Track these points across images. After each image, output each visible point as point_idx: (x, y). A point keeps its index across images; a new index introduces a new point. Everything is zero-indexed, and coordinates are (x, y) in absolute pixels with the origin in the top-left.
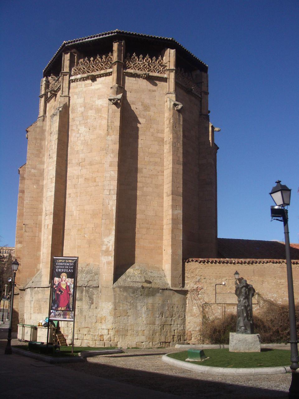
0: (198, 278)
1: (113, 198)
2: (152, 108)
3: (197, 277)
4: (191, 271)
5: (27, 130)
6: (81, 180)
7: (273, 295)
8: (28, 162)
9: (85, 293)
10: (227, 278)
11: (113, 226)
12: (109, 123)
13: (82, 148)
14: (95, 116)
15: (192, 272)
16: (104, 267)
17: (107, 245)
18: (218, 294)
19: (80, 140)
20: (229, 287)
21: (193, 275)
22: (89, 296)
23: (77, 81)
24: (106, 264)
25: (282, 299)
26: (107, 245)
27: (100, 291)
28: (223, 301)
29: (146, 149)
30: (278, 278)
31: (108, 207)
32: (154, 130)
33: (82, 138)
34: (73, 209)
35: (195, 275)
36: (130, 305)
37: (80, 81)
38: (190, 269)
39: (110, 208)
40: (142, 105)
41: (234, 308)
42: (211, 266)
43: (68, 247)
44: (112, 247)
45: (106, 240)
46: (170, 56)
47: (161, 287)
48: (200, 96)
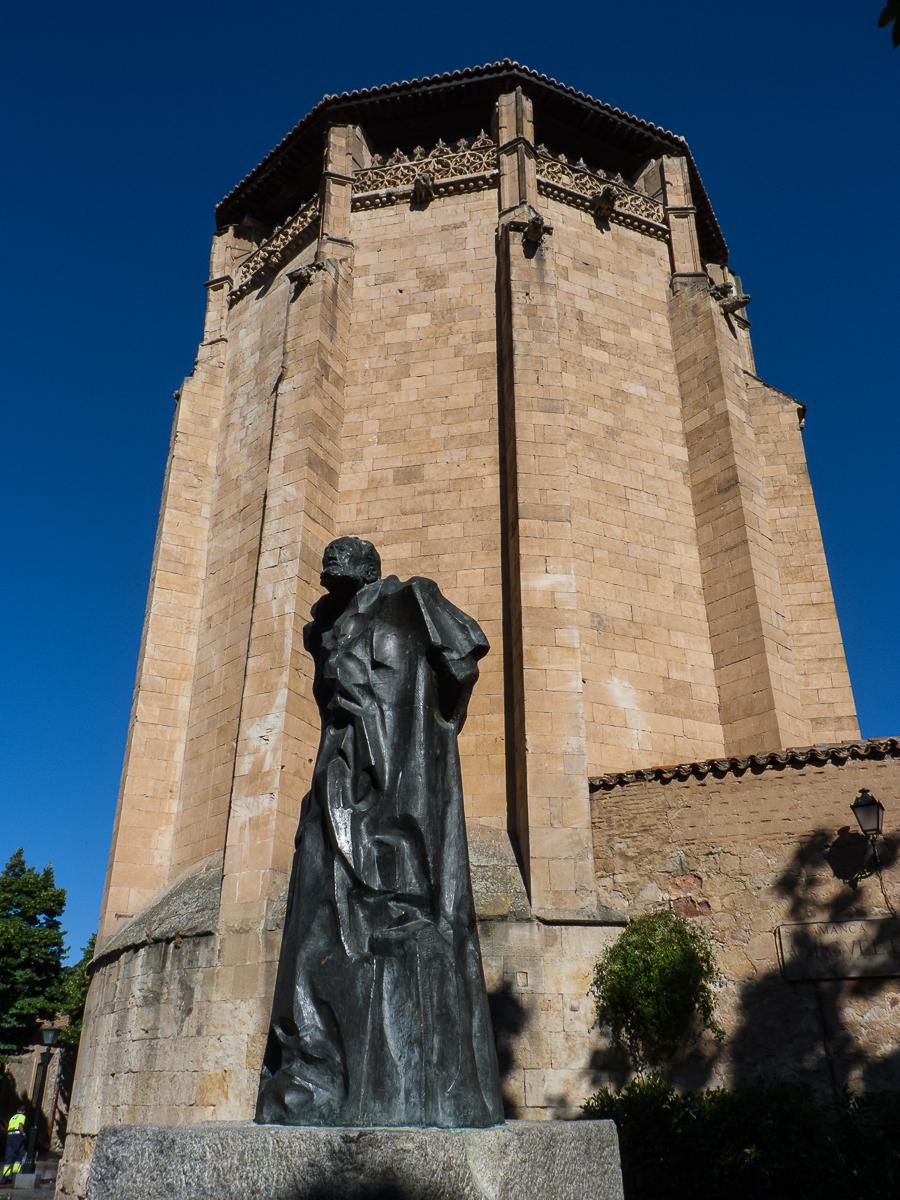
0: (678, 853)
2: (453, 276)
3: (668, 849)
9: (173, 965)
16: (240, 841)
17: (257, 751)
21: (648, 845)
22: (180, 981)
24: (247, 828)
26: (257, 751)
27: (220, 951)
29: (433, 401)
31: (270, 608)
35: (658, 843)
42: (737, 790)
46: (513, 113)
48: (665, 227)
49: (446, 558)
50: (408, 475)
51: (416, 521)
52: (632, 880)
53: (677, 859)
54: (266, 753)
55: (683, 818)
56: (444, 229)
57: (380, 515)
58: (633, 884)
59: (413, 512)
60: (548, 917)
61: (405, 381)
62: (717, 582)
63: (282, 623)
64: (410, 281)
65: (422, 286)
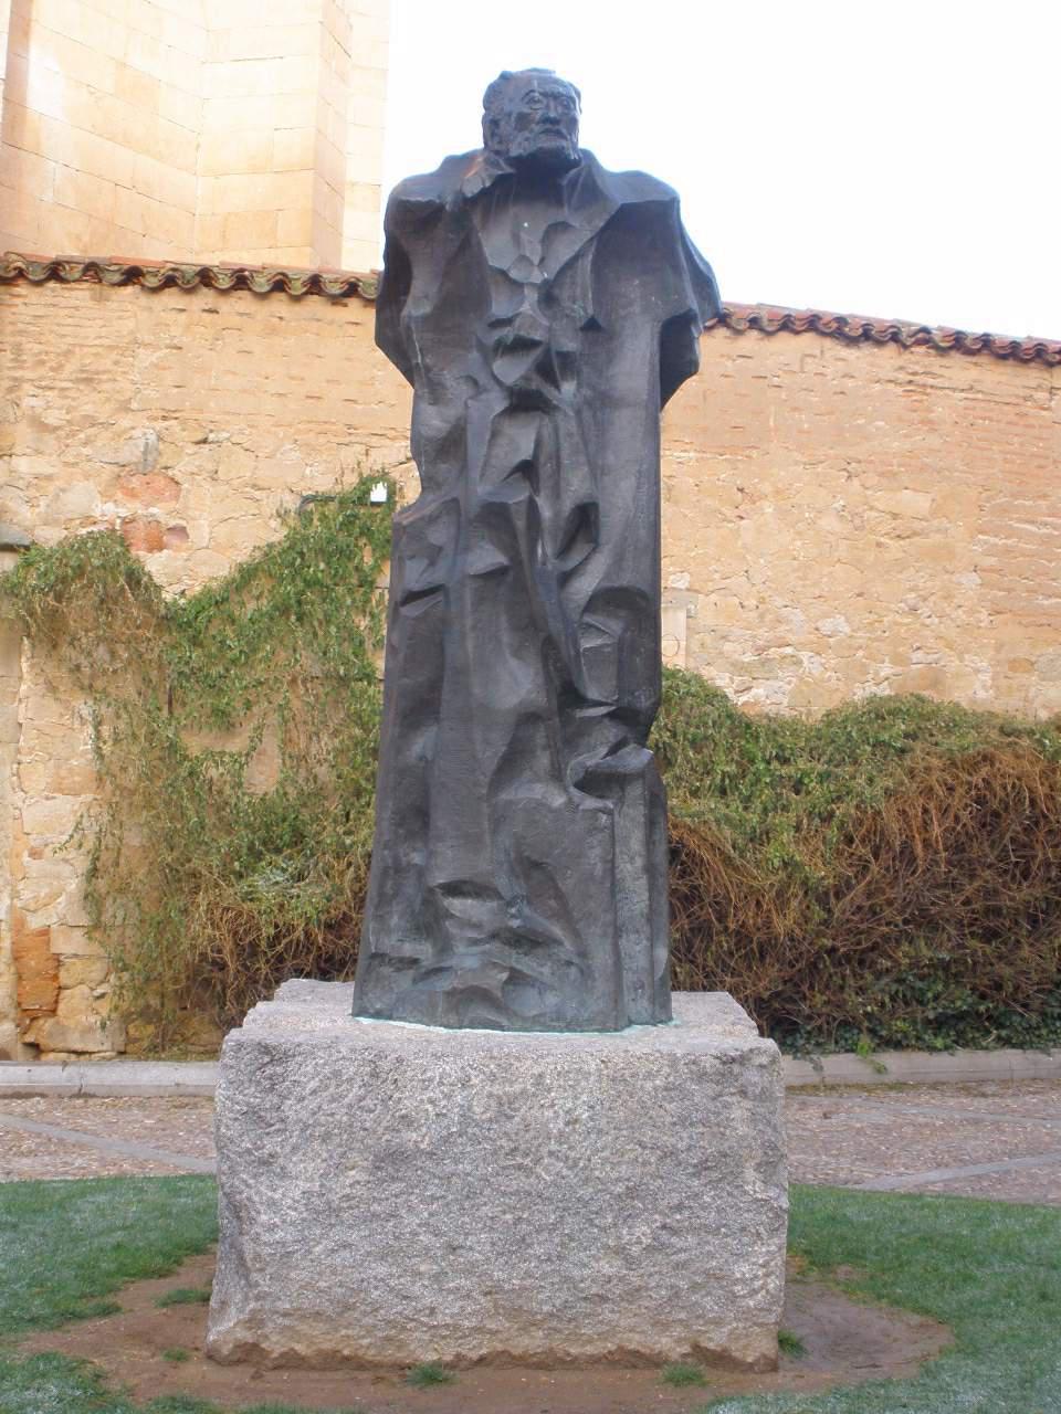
0: (144, 432)
3: (125, 421)
4: (71, 367)
7: (826, 626)
15: (88, 381)
21: (88, 409)
25: (898, 660)
30: (873, 480)
35: (109, 407)
38: (68, 353)
42: (273, 331)
52: (48, 470)
53: (141, 443)
55: (164, 369)
58: (49, 478)
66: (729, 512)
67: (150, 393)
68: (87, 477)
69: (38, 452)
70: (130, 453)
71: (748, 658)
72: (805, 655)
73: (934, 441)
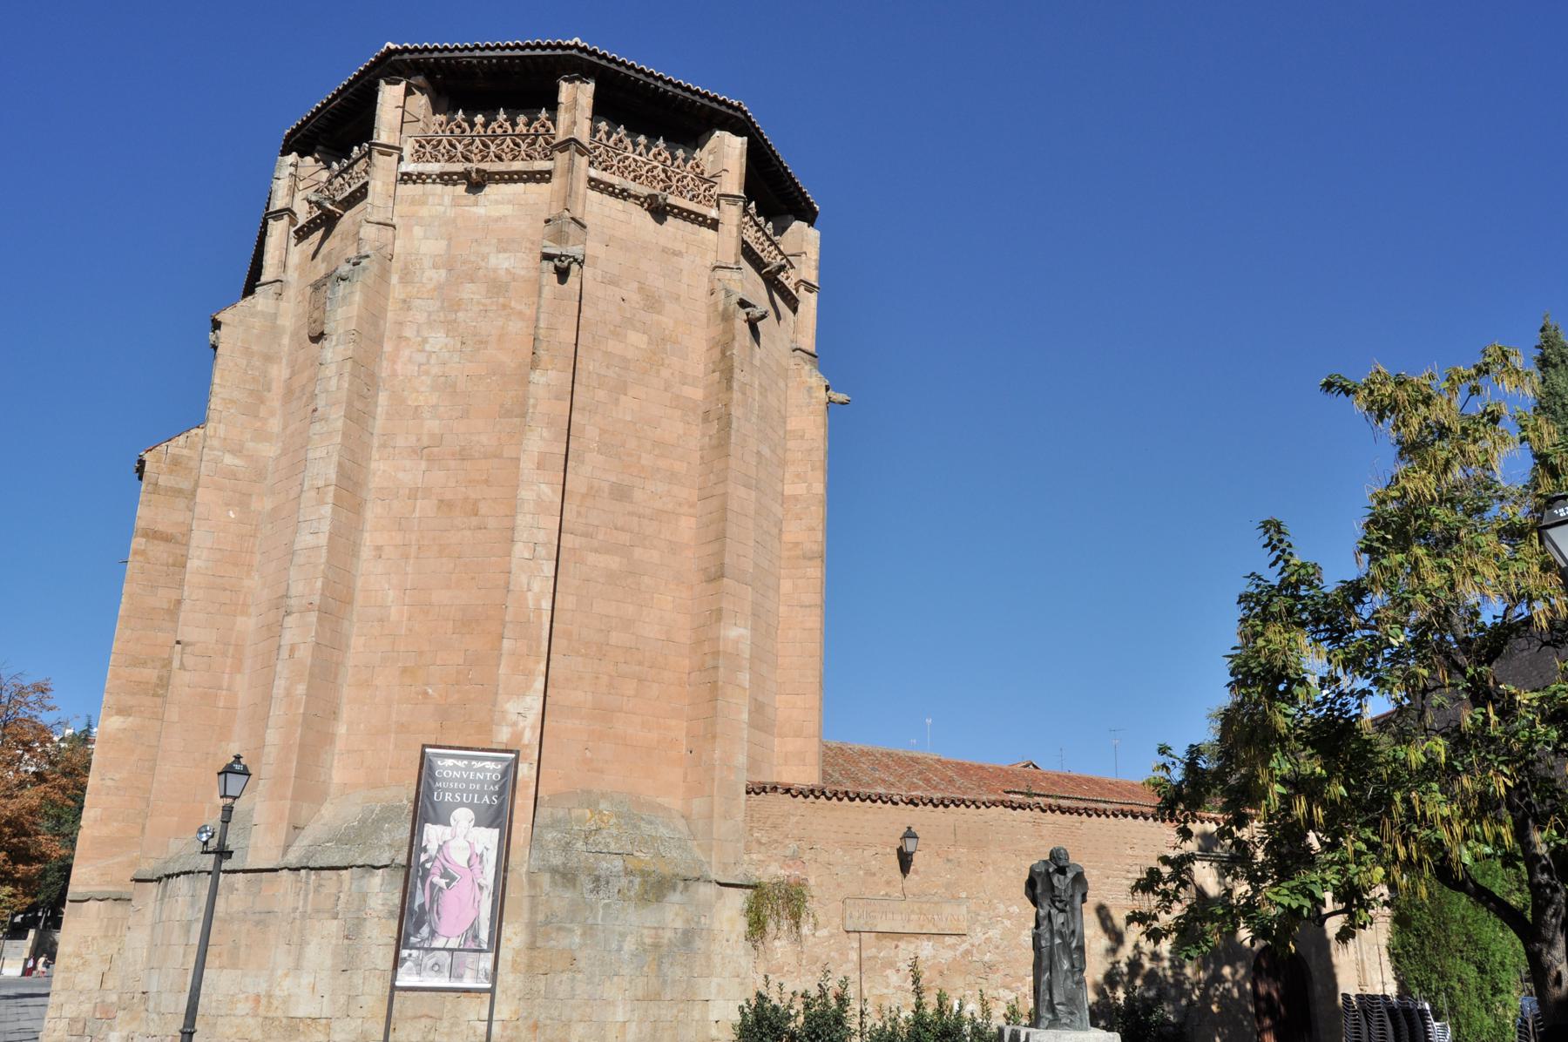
0: (793, 845)
1: (542, 571)
3: (787, 841)
4: (769, 823)
5: (219, 317)
6: (425, 507)
7: (1011, 909)
8: (212, 430)
10: (879, 849)
11: (538, 663)
12: (541, 331)
13: (433, 399)
14: (485, 305)
17: (515, 724)
18: (852, 901)
19: (427, 373)
20: (884, 879)
21: (775, 837)
23: (424, 182)
26: (515, 724)
28: (866, 923)
32: (673, 374)
33: (435, 370)
34: (390, 599)
35: (782, 837)
36: (584, 934)
37: (434, 182)
38: (768, 818)
39: (531, 603)
40: (641, 289)
41: (897, 947)
43: (362, 726)
44: (533, 734)
45: (511, 707)
47: (683, 872)
49: (646, 579)
50: (621, 493)
51: (624, 538)
52: (762, 858)
54: (524, 728)
56: (664, 250)
57: (596, 523)
58: (763, 861)
59: (622, 530)
60: (722, 881)
61: (623, 398)
62: (790, 628)
63: (540, 617)
64: (630, 291)
65: (642, 303)
66: (978, 870)
67: (795, 832)
68: (776, 861)
69: (759, 852)
70: (789, 852)
71: (986, 922)
72: (1005, 921)
73: (1043, 842)
